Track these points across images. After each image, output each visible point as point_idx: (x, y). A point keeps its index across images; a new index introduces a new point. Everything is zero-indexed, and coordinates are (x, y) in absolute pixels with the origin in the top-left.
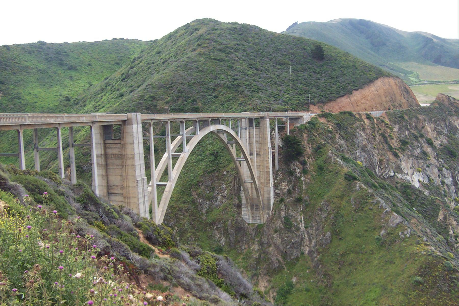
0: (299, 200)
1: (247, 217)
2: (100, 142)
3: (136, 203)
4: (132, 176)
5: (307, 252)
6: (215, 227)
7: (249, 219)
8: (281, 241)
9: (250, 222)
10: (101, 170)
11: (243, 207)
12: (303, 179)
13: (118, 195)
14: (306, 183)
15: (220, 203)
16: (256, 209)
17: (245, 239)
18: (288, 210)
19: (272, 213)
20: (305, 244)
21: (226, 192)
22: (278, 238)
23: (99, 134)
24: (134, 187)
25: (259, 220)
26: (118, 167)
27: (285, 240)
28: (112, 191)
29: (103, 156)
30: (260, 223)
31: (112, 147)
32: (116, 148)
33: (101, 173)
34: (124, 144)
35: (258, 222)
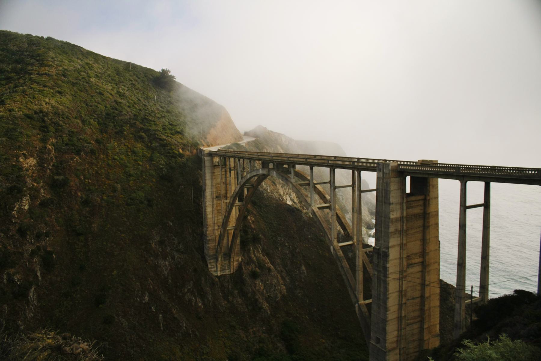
0: (256, 240)
1: (215, 269)
2: (400, 201)
3: (437, 269)
4: (435, 237)
5: (285, 291)
6: (186, 290)
7: (217, 271)
8: (263, 286)
9: (219, 274)
10: (399, 238)
11: (210, 259)
12: (249, 218)
13: (415, 265)
14: (253, 222)
15: (179, 260)
16: (224, 258)
17: (221, 294)
18: (254, 252)
19: (241, 259)
20: (280, 283)
21: (181, 246)
22: (261, 284)
23: (400, 190)
24: (437, 250)
25: (228, 269)
26: (418, 230)
27: (268, 284)
28: (410, 262)
29: (405, 219)
30: (229, 273)
31: (414, 205)
32: (418, 205)
33: (399, 242)
34: (430, 199)
35: (227, 272)
